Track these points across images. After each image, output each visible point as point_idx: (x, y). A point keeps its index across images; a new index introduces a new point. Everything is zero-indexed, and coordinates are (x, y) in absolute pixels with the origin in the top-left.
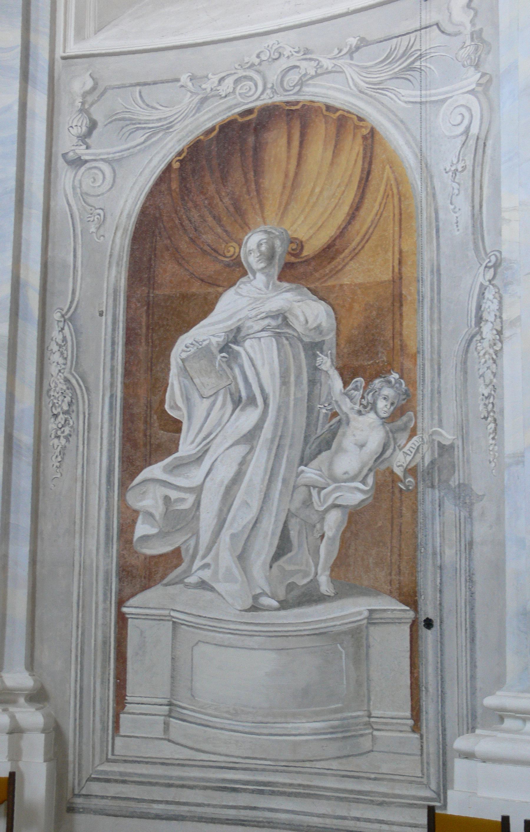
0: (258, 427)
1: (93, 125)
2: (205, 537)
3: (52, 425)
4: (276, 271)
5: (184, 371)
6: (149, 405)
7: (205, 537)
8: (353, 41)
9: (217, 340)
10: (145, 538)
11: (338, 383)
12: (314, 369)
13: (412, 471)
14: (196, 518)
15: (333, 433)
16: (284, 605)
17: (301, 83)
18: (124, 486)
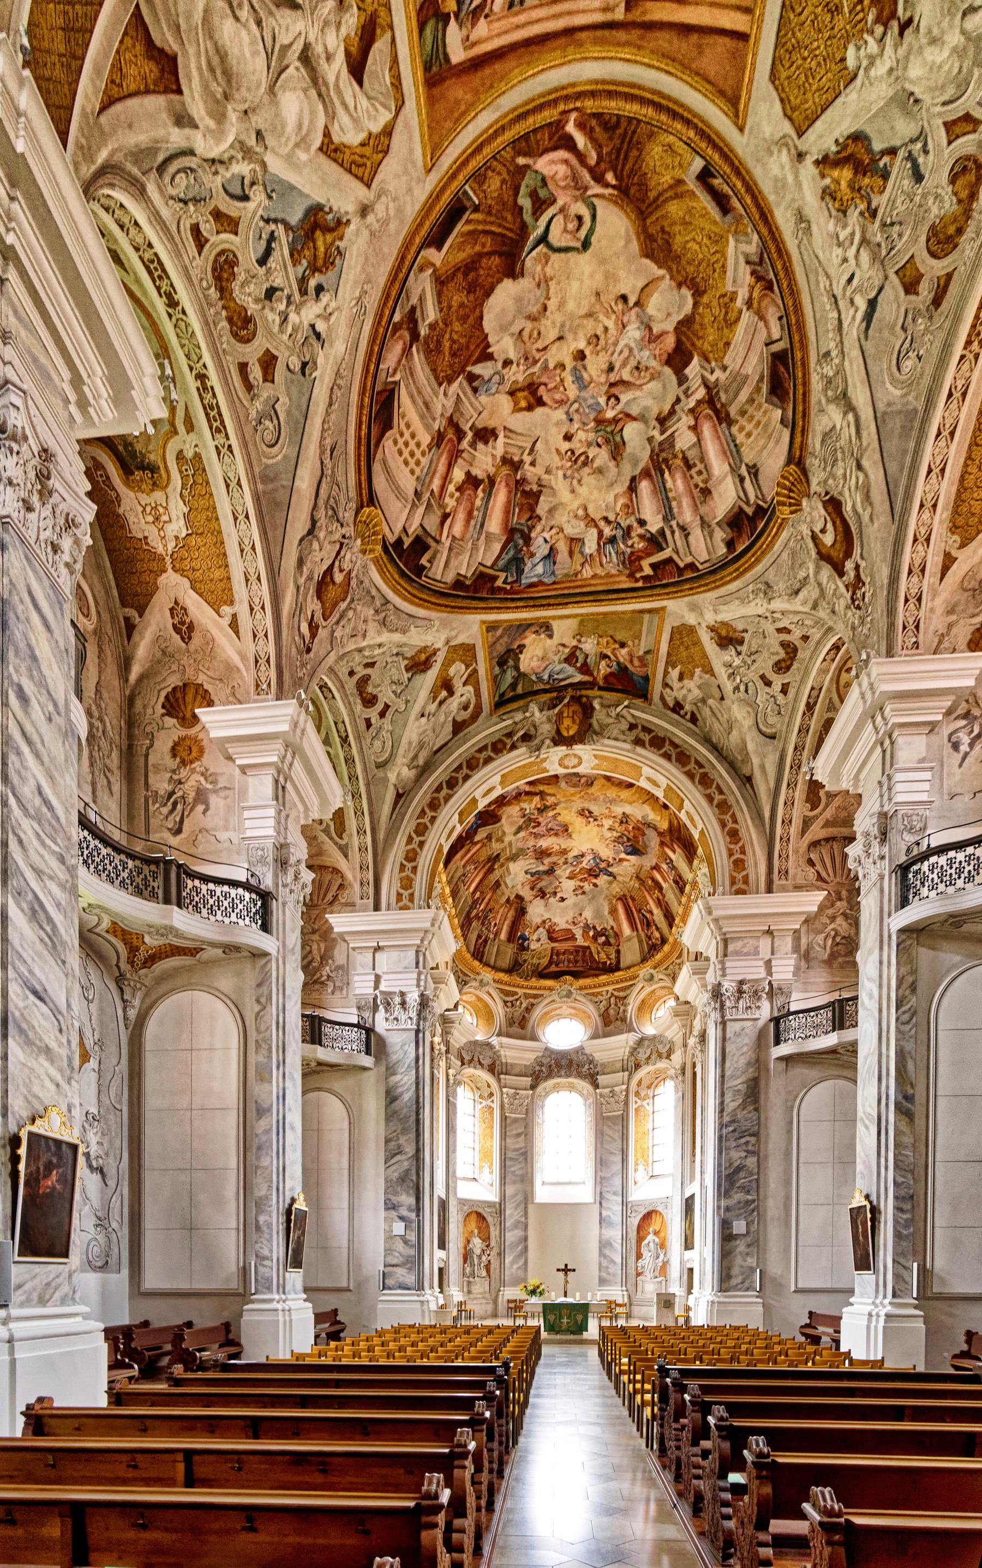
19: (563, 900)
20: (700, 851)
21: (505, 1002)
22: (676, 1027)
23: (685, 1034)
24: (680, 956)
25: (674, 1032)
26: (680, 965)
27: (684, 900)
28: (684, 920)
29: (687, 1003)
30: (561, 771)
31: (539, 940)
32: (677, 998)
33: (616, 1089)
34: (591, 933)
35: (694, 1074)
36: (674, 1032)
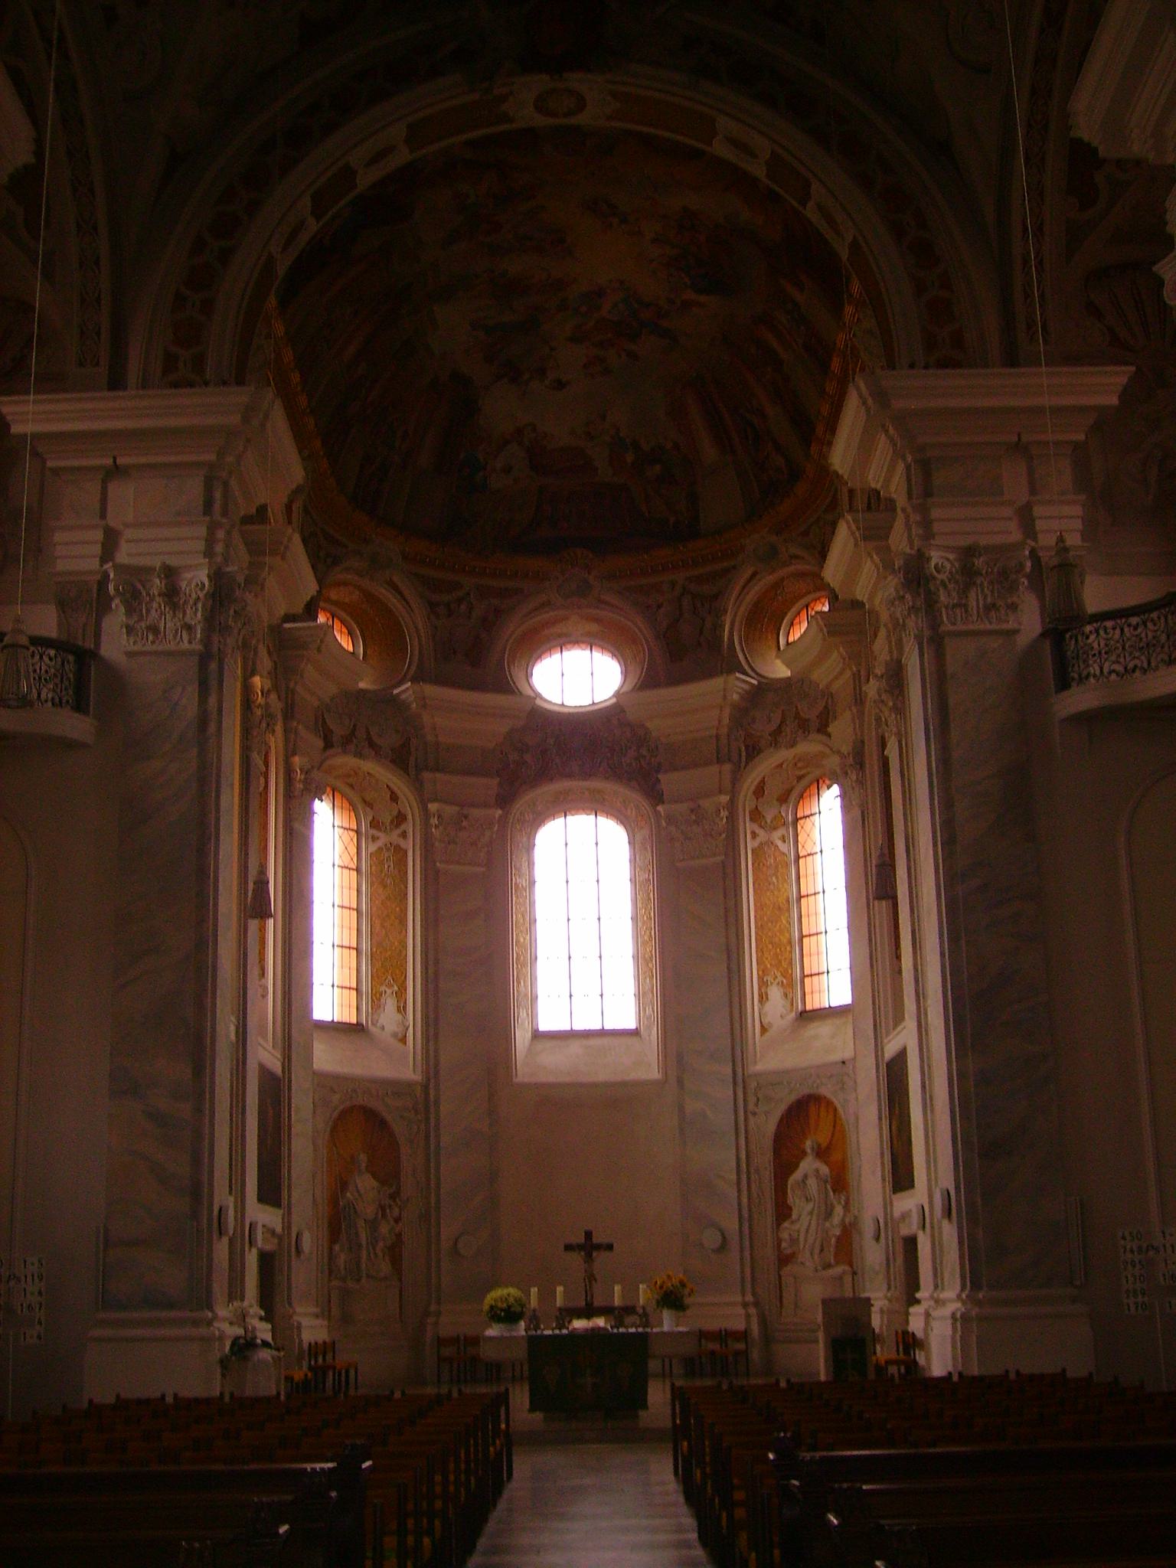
0: (813, 1209)
1: (758, 1099)
2: (802, 1247)
3: (754, 1210)
4: (814, 1154)
5: (793, 1190)
6: (783, 1202)
7: (802, 1247)
8: (829, 1074)
9: (800, 1179)
10: (785, 1249)
11: (832, 1193)
12: (826, 1188)
13: (850, 1224)
14: (798, 1239)
15: (832, 1210)
16: (824, 1269)
17: (817, 1087)
18: (777, 1232)
19: (560, 385)
20: (856, 287)
21: (432, 606)
22: (834, 660)
23: (856, 676)
24: (834, 505)
25: (831, 672)
26: (834, 525)
27: (830, 387)
28: (832, 427)
29: (857, 605)
30: (541, 121)
31: (508, 470)
32: (834, 598)
33: (707, 804)
34: (630, 458)
35: (885, 763)
36: (831, 672)
